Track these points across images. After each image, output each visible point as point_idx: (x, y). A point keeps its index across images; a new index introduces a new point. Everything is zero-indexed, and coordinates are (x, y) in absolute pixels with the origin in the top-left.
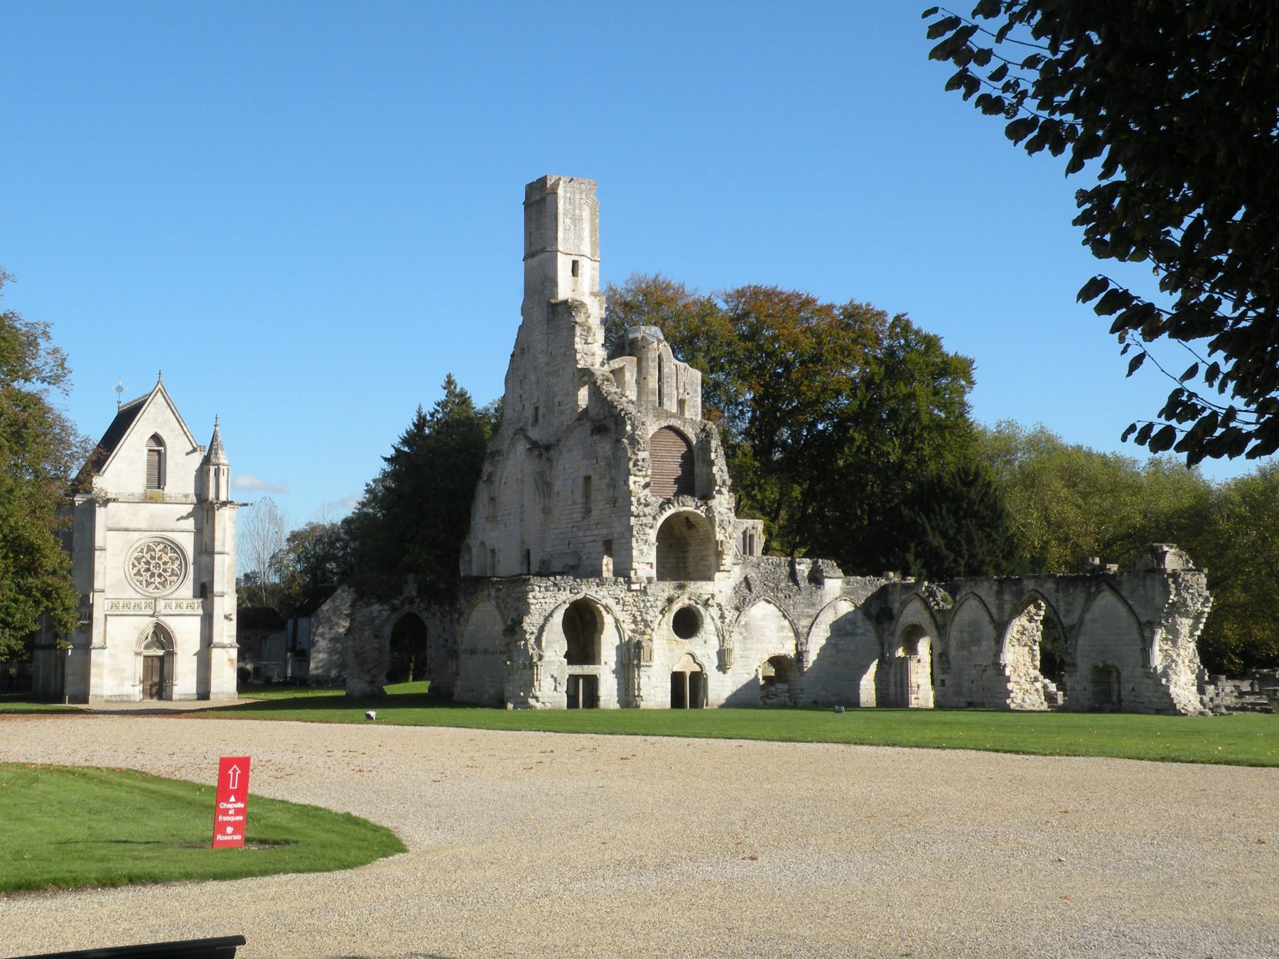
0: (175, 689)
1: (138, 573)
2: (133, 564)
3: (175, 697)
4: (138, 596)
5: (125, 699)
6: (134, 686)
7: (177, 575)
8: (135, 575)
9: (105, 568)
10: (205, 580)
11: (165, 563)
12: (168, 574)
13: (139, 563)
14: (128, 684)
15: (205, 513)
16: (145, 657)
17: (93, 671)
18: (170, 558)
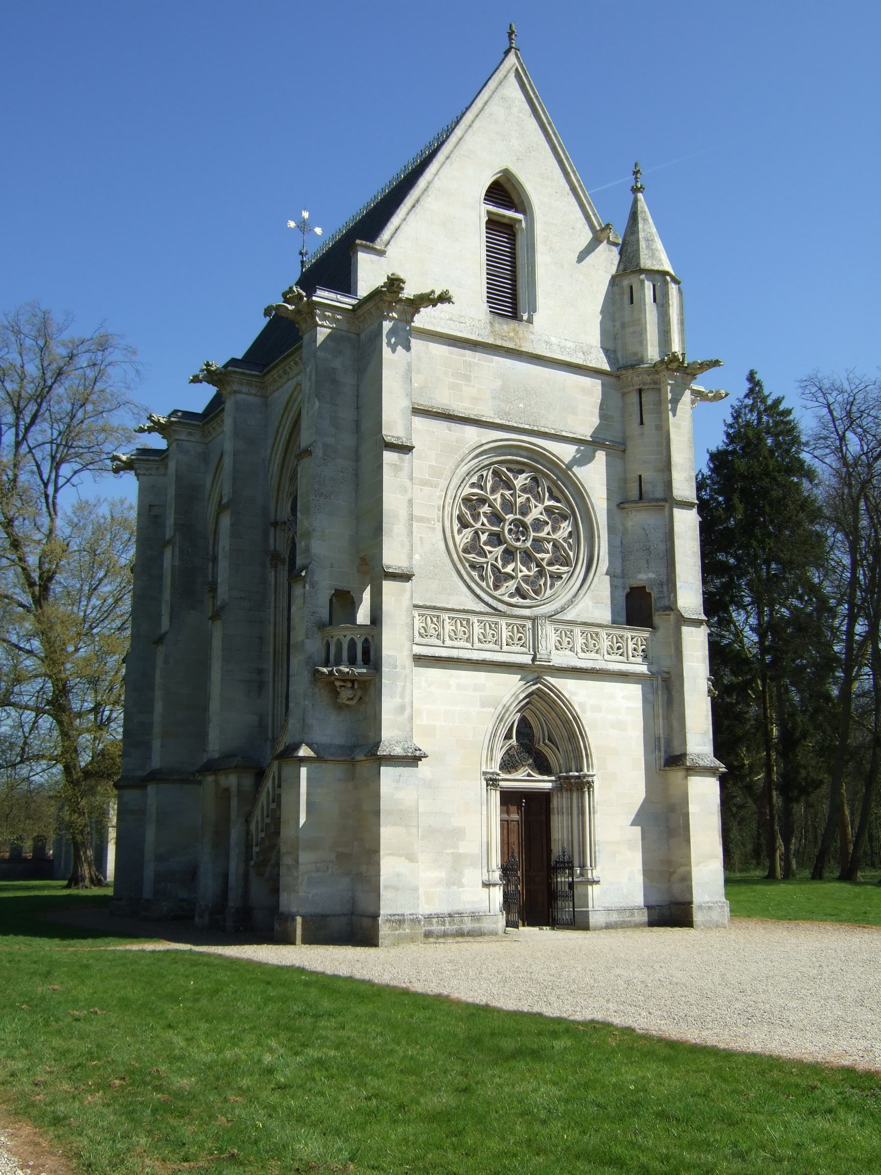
0: (594, 892)
1: (473, 547)
2: (460, 518)
3: (595, 919)
4: (481, 607)
5: (468, 925)
6: (487, 885)
7: (566, 562)
8: (465, 551)
9: (410, 502)
10: (643, 578)
11: (538, 525)
12: (547, 556)
13: (476, 517)
14: (474, 876)
15: (634, 398)
16: (509, 798)
17: (388, 833)
18: (548, 510)
